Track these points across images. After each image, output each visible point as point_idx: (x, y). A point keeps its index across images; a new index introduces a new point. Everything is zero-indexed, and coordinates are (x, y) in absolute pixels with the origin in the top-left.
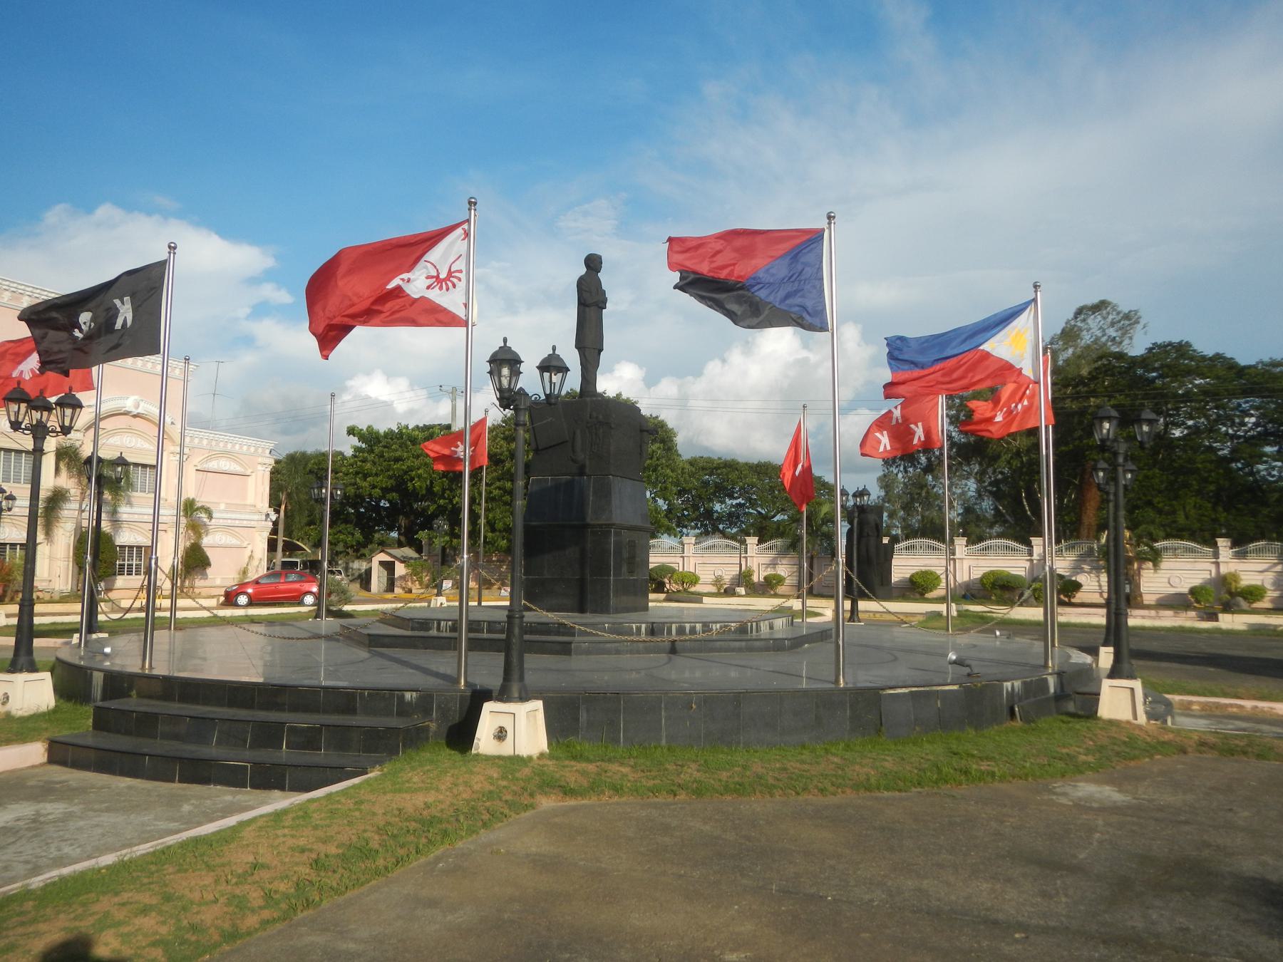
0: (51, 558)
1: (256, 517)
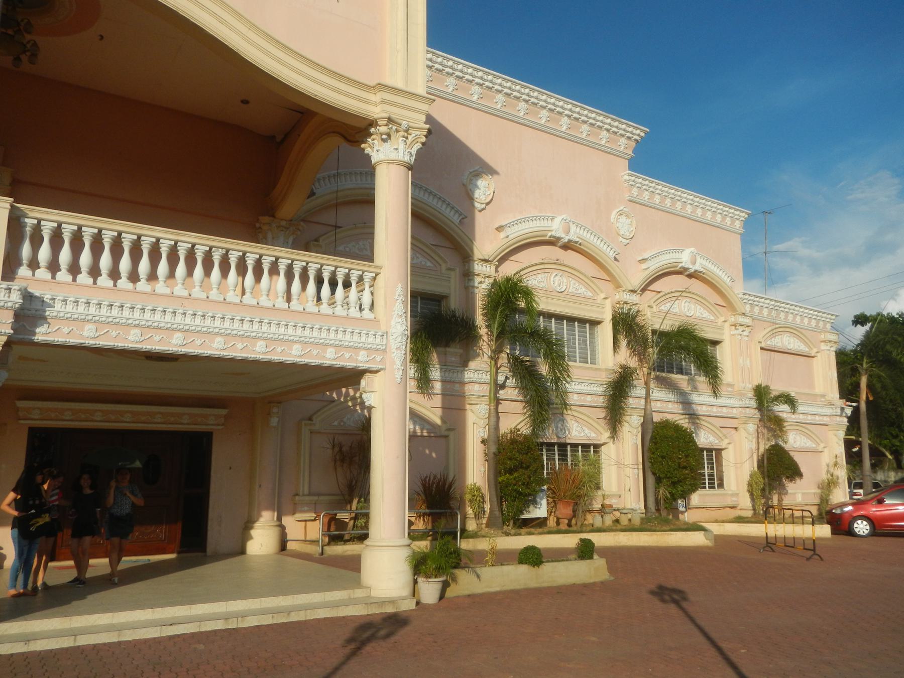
0: (619, 464)
1: (829, 411)
